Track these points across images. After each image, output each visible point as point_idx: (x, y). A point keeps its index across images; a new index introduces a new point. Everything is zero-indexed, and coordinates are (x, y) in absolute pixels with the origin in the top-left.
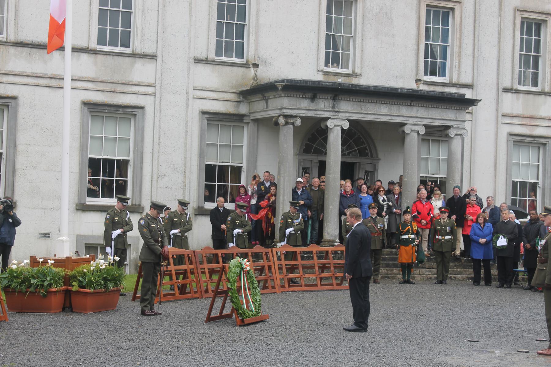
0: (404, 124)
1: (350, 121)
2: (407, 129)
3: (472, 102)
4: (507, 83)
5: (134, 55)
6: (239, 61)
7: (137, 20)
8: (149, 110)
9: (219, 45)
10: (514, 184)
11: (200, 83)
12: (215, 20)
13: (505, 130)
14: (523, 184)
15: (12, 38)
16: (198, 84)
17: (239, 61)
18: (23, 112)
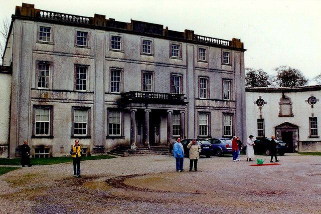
0: (167, 110)
1: (151, 109)
2: (168, 111)
3: (187, 103)
4: (197, 97)
5: (87, 92)
6: (118, 93)
7: (88, 83)
8: (92, 108)
9: (112, 88)
10: (200, 126)
11: (107, 100)
12: (111, 81)
13: (197, 110)
14: (203, 126)
15: (51, 89)
16: (107, 100)
17: (118, 93)
18: (55, 110)
